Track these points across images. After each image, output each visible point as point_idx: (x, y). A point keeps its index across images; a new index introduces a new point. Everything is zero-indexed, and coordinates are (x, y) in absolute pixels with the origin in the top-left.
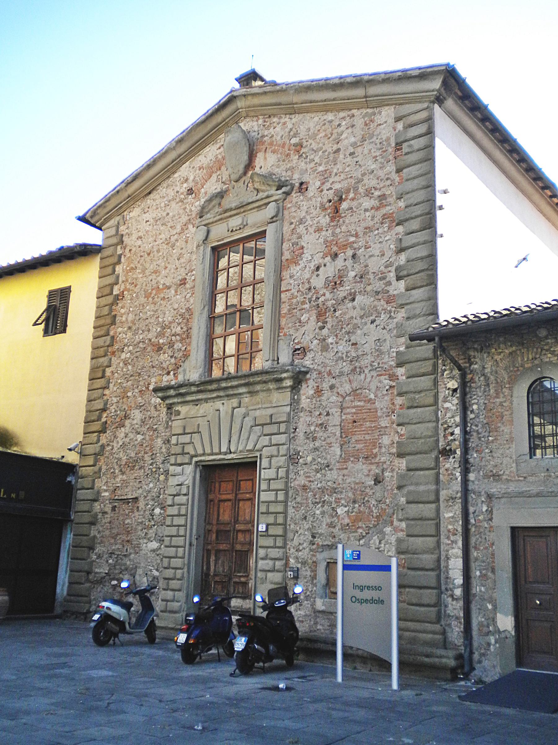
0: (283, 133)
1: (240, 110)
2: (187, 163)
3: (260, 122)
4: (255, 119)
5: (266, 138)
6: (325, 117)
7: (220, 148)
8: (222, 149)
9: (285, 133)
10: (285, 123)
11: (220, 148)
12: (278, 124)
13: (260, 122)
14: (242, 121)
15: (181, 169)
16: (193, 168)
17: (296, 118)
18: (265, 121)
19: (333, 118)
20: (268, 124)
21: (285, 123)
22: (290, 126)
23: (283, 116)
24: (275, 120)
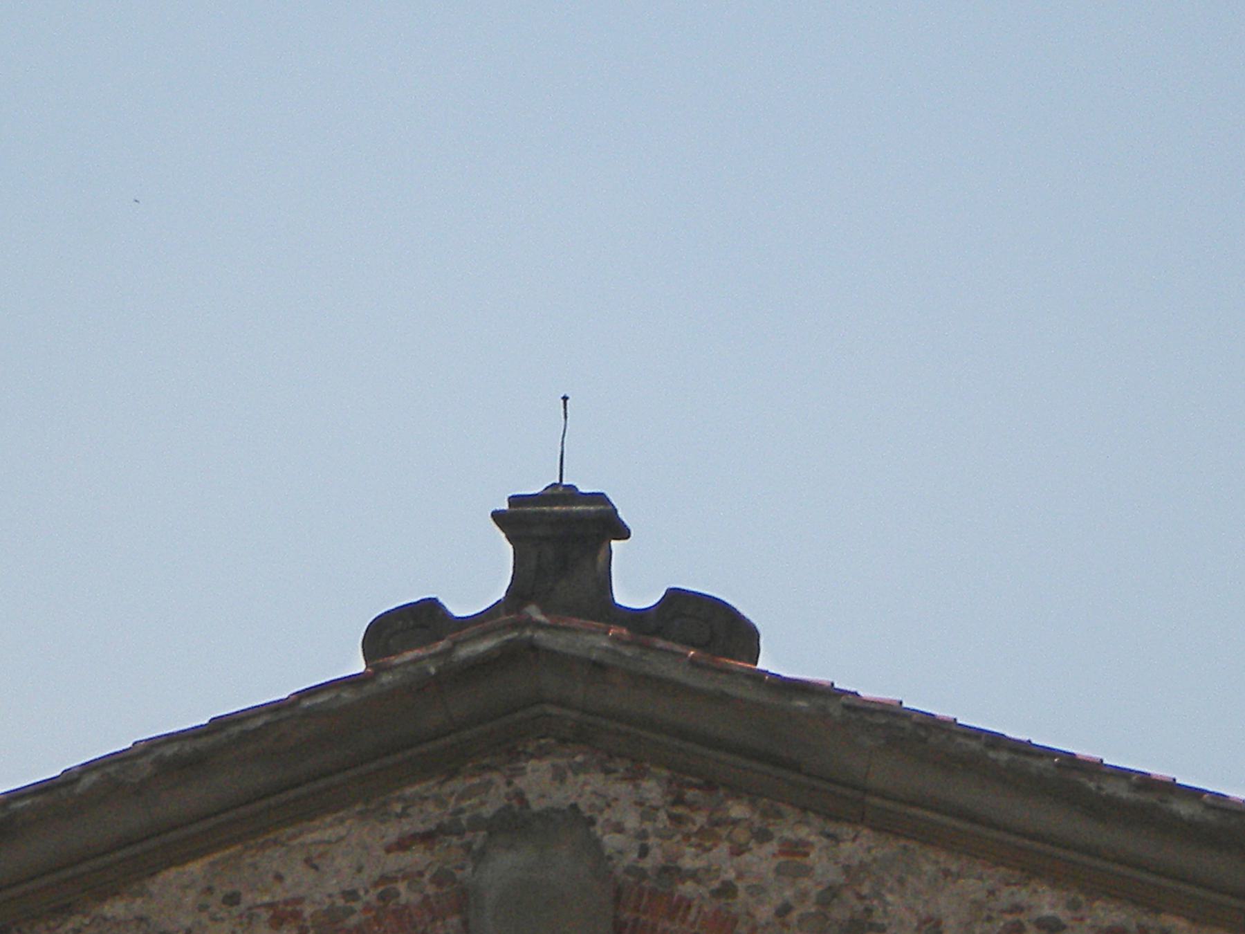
0: (788, 893)
1: (553, 710)
2: (196, 867)
3: (652, 790)
4: (621, 766)
5: (688, 888)
6: (1023, 895)
7: (402, 845)
8: (416, 857)
9: (803, 896)
10: (796, 849)
11: (402, 845)
12: (763, 836)
13: (652, 790)
14: (541, 754)
15: (154, 886)
16: (232, 899)
17: (859, 846)
18: (679, 801)
19: (1063, 914)
20: (701, 819)
21: (796, 849)
22: (822, 867)
23: (791, 813)
24: (737, 810)
